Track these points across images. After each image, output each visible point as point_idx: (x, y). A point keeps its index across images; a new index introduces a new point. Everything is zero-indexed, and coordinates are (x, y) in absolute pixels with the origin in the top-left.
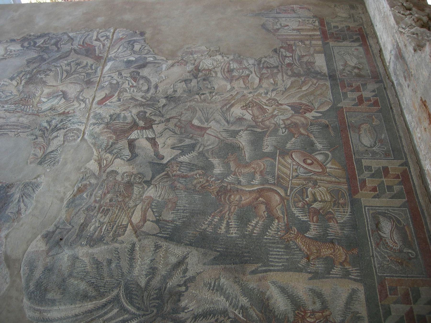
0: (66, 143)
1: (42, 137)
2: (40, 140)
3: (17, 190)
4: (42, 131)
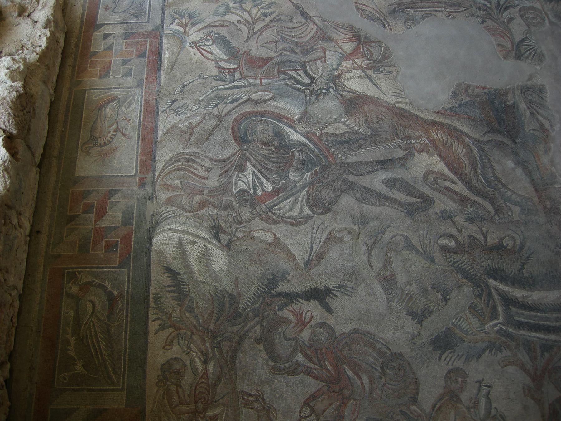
0: (533, 29)
1: (489, 19)
2: (489, 23)
3: (517, 98)
4: (484, 10)
